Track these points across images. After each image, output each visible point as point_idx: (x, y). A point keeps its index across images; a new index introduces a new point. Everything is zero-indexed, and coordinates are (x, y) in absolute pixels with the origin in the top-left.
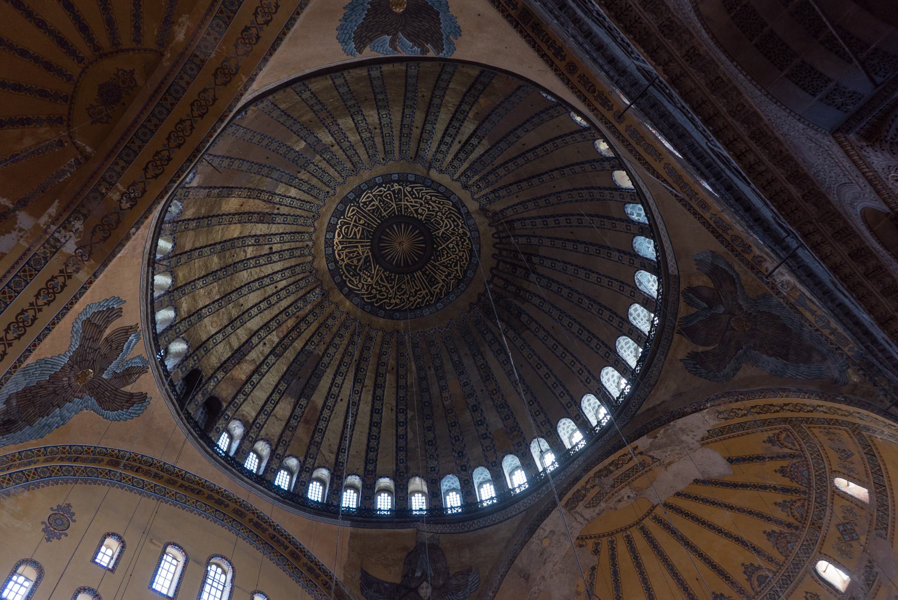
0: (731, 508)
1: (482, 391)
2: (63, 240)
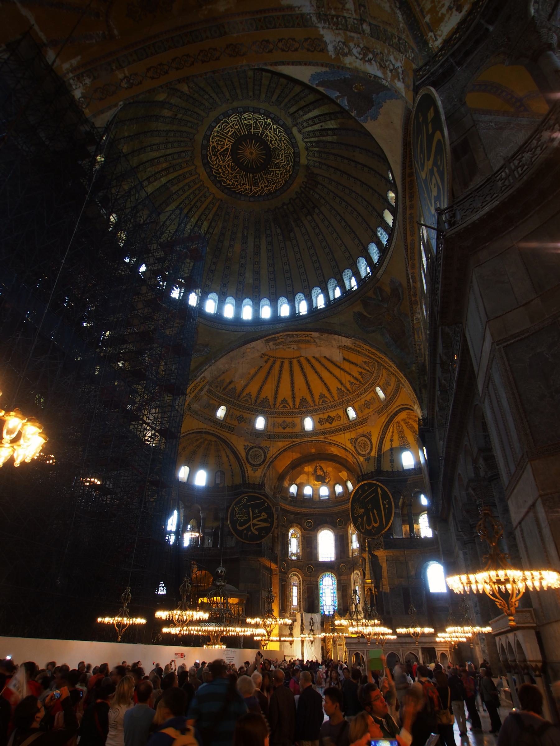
0: (331, 373)
1: (250, 258)
2: (74, 87)
